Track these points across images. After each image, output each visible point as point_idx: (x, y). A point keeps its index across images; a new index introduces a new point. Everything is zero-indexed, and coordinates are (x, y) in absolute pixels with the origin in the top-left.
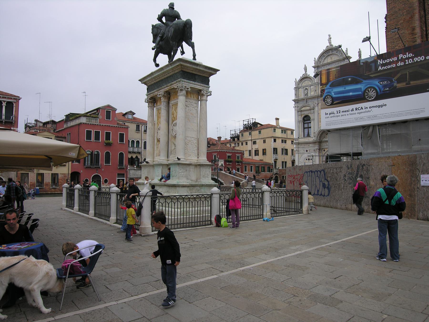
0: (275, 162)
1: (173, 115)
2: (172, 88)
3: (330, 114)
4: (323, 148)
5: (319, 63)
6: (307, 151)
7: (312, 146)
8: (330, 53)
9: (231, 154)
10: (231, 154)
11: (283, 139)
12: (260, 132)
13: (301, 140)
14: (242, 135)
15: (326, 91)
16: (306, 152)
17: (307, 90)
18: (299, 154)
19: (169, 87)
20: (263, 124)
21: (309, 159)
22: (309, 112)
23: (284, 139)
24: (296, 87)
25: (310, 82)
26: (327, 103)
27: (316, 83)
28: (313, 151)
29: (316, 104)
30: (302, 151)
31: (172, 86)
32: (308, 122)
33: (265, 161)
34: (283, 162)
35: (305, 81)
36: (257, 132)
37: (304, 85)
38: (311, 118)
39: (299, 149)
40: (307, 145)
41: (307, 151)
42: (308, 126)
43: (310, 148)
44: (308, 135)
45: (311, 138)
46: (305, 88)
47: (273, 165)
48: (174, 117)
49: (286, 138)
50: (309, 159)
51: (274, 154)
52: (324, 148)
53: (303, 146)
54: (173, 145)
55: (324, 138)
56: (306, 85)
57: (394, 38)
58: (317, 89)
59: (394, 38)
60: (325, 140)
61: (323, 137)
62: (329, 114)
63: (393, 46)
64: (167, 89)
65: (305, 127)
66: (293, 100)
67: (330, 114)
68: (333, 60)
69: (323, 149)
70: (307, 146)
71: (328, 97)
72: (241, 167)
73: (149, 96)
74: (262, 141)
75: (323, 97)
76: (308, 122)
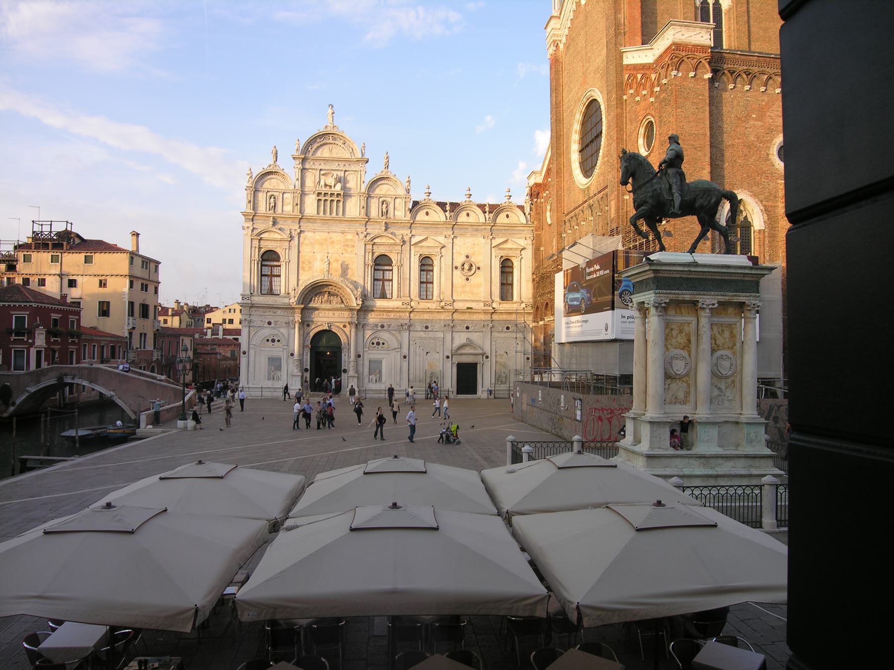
0: (130, 334)
1: (716, 340)
2: (735, 301)
3: (628, 318)
4: (305, 321)
5: (306, 153)
6: (269, 323)
7: (282, 314)
8: (331, 141)
9: (60, 316)
10: (60, 316)
11: (144, 281)
12: (88, 260)
13: (258, 299)
14: (27, 259)
15: (624, 284)
16: (266, 325)
17: (275, 198)
18: (251, 328)
19: (727, 298)
20: (85, 238)
21: (273, 341)
22: (279, 244)
23: (145, 282)
24: (251, 187)
25: (282, 184)
26: (625, 302)
27: (297, 190)
28: (284, 325)
29: (296, 233)
30: (258, 323)
31: (735, 298)
32: (276, 263)
33: (101, 328)
34: (141, 334)
35: (271, 179)
36: (81, 257)
37: (269, 187)
38: (282, 259)
39: (252, 317)
40: (270, 311)
41: (269, 323)
42: (271, 273)
43: (277, 319)
44: (271, 292)
45: (281, 297)
46: (269, 194)
47: (127, 342)
48: (715, 343)
49: (148, 279)
50: (273, 341)
51: (129, 315)
52: (308, 321)
53: (260, 312)
54: (716, 389)
55: (311, 301)
56: (272, 187)
57: (683, 230)
58: (299, 203)
59: (683, 230)
60: (314, 305)
61: (308, 300)
62: (626, 317)
63: (682, 240)
64: (722, 298)
65: (263, 273)
66: (241, 212)
67: (628, 318)
68: (334, 155)
69: (306, 323)
70: (271, 314)
71: (626, 293)
72: (76, 349)
73: (661, 295)
74: (96, 281)
75: (620, 291)
76: (276, 263)
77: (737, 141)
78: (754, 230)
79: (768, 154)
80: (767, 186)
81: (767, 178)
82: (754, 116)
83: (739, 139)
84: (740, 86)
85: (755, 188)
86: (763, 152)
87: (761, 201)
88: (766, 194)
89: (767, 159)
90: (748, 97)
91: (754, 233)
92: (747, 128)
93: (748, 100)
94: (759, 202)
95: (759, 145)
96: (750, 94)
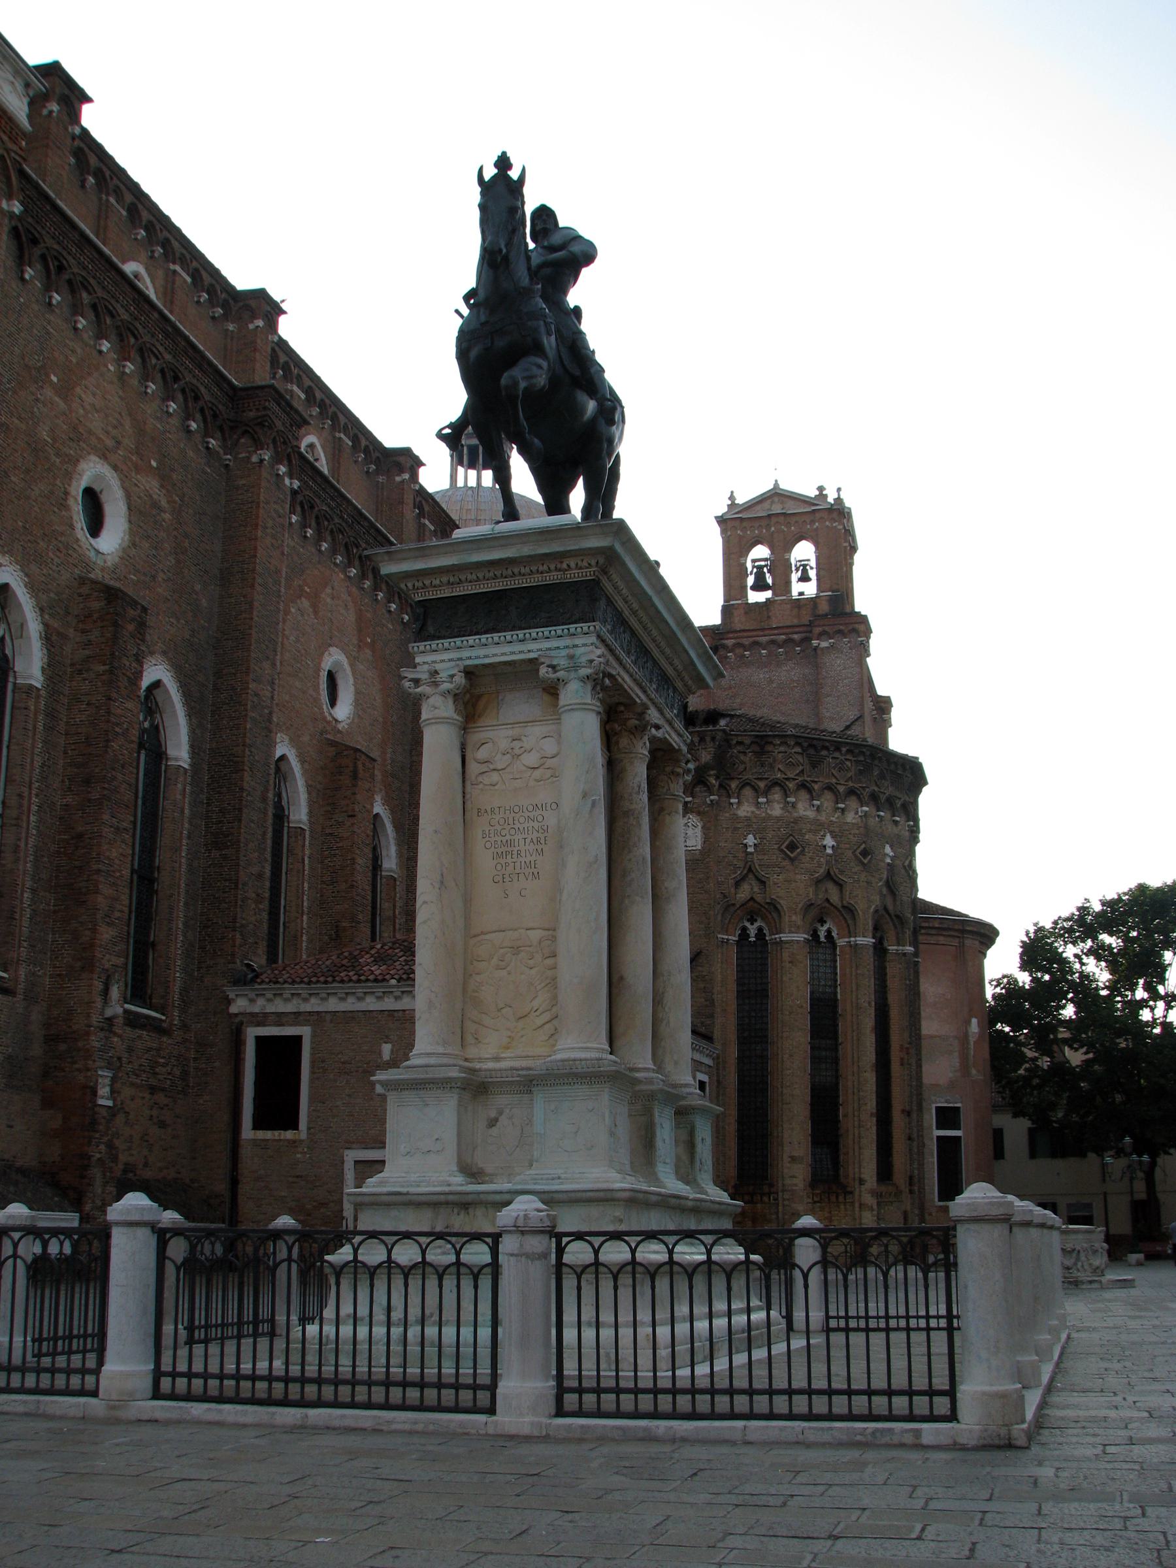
77: (16, 421)
78: (15, 684)
79: (67, 493)
80: (56, 575)
81: (58, 553)
82: (54, 379)
83: (20, 418)
84: (39, 285)
85: (34, 568)
86: (58, 482)
87: (42, 610)
88: (52, 595)
89: (63, 505)
90: (49, 323)
91: (14, 692)
92: (37, 400)
93: (48, 333)
94: (37, 610)
95: (53, 458)
96: (52, 318)
